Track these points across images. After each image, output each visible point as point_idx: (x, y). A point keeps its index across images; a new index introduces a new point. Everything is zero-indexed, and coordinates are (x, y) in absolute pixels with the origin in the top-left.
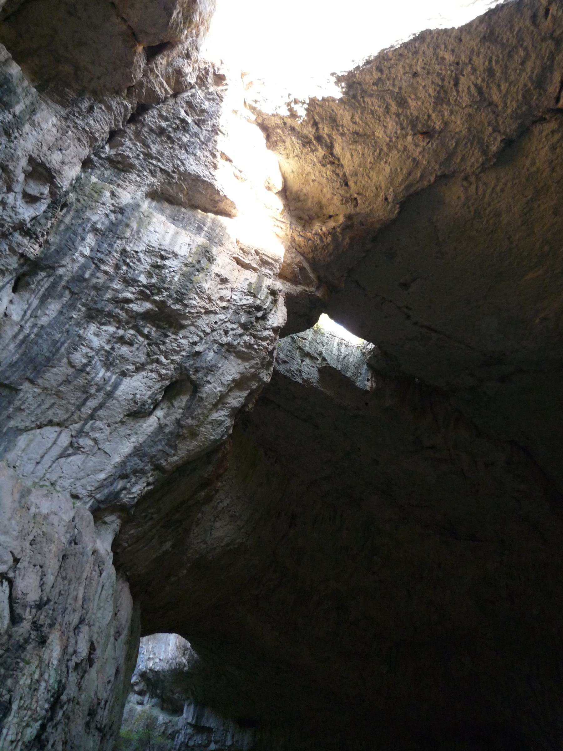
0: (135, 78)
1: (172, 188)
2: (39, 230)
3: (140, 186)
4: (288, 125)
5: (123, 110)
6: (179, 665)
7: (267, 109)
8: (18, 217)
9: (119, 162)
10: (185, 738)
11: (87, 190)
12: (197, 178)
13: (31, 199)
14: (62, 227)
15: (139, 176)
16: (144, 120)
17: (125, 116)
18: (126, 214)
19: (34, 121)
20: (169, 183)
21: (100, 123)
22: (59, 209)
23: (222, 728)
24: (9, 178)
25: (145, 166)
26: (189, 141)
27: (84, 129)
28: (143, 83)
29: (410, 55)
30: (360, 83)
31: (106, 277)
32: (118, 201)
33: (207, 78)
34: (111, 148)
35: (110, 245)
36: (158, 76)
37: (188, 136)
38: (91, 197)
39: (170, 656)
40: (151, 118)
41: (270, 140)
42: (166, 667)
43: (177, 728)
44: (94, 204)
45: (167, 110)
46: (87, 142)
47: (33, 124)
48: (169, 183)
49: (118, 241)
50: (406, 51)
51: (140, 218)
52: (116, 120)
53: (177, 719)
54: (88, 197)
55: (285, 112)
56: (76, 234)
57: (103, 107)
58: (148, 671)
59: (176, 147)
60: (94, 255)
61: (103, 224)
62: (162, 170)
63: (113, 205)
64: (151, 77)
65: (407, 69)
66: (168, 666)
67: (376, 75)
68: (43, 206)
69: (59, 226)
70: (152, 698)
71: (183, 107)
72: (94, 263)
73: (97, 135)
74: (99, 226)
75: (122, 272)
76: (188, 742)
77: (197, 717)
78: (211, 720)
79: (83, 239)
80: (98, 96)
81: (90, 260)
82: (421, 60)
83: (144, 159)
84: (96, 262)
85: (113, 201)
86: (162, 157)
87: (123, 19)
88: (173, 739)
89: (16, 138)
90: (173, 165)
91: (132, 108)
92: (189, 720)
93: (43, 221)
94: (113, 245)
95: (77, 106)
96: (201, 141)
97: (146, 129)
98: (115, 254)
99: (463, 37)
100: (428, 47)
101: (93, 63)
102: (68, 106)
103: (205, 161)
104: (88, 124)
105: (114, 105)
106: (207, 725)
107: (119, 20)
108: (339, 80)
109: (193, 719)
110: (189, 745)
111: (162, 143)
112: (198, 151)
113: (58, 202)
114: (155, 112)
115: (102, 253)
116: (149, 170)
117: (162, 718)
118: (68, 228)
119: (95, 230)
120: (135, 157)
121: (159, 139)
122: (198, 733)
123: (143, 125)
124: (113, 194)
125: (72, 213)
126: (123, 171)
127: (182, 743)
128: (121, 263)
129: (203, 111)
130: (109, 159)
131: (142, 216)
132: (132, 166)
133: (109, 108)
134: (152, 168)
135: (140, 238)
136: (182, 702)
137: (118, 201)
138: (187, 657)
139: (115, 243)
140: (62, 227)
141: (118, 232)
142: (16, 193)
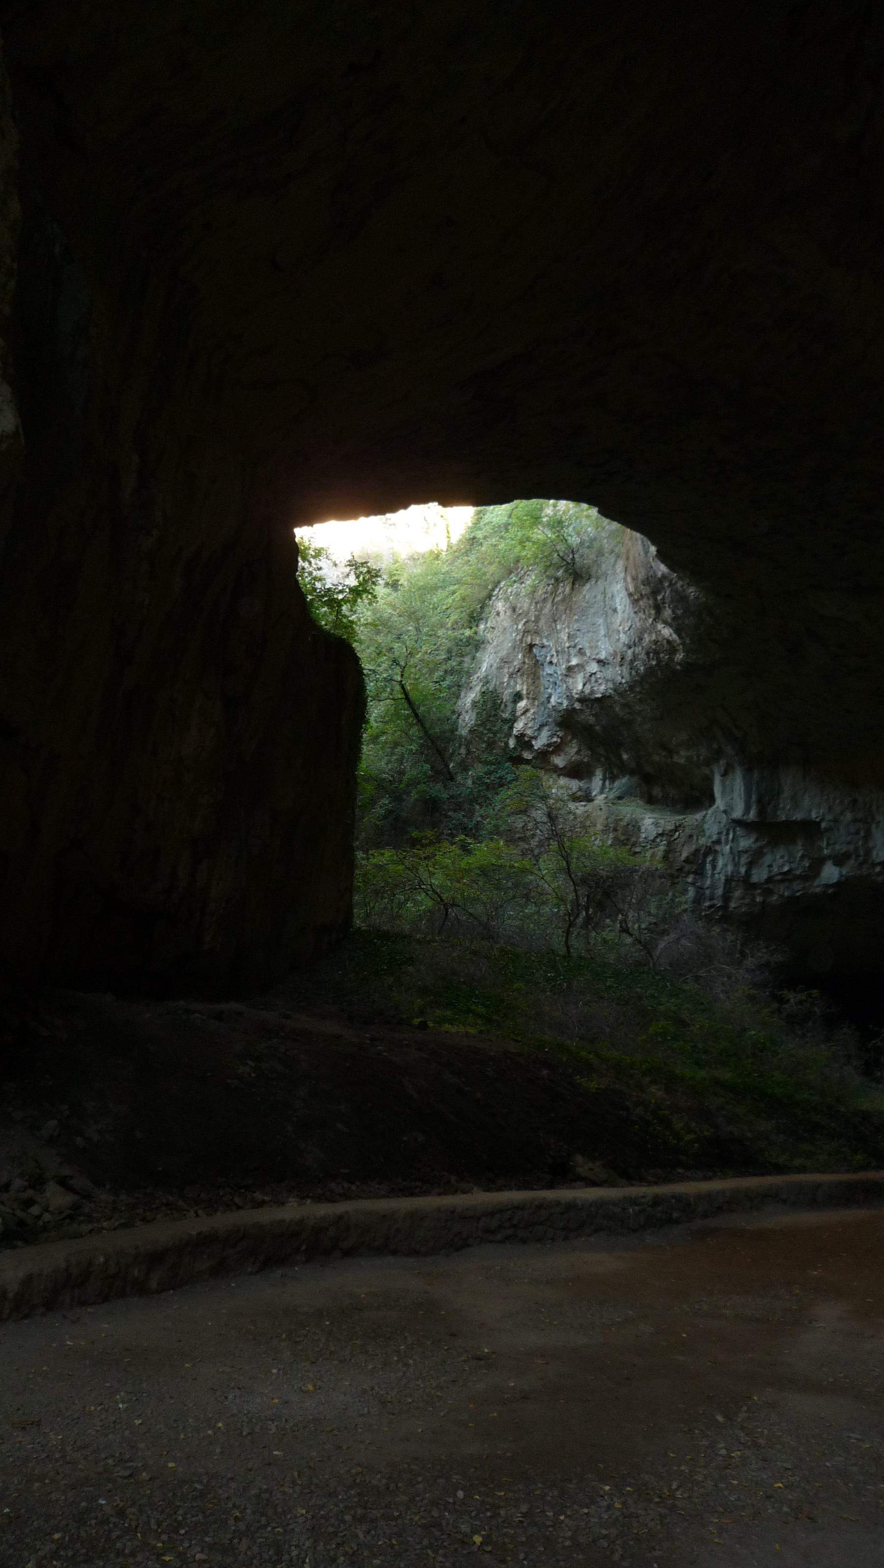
6: (656, 653)
10: (736, 865)
23: (849, 816)
39: (623, 638)
42: (618, 674)
43: (703, 841)
53: (698, 816)
58: (577, 706)
66: (625, 670)
70: (613, 779)
76: (748, 874)
77: (759, 801)
78: (806, 802)
88: (700, 872)
92: (738, 814)
106: (798, 816)
109: (747, 809)
110: (755, 879)
117: (651, 823)
122: (774, 843)
127: (728, 881)
136: (706, 771)
138: (667, 613)
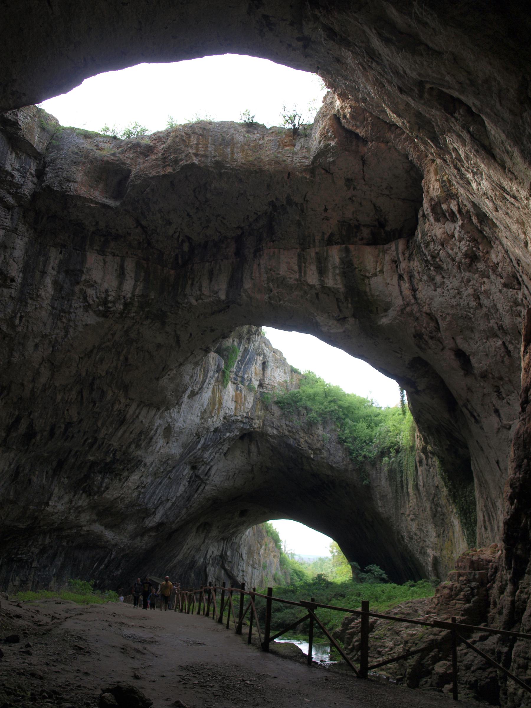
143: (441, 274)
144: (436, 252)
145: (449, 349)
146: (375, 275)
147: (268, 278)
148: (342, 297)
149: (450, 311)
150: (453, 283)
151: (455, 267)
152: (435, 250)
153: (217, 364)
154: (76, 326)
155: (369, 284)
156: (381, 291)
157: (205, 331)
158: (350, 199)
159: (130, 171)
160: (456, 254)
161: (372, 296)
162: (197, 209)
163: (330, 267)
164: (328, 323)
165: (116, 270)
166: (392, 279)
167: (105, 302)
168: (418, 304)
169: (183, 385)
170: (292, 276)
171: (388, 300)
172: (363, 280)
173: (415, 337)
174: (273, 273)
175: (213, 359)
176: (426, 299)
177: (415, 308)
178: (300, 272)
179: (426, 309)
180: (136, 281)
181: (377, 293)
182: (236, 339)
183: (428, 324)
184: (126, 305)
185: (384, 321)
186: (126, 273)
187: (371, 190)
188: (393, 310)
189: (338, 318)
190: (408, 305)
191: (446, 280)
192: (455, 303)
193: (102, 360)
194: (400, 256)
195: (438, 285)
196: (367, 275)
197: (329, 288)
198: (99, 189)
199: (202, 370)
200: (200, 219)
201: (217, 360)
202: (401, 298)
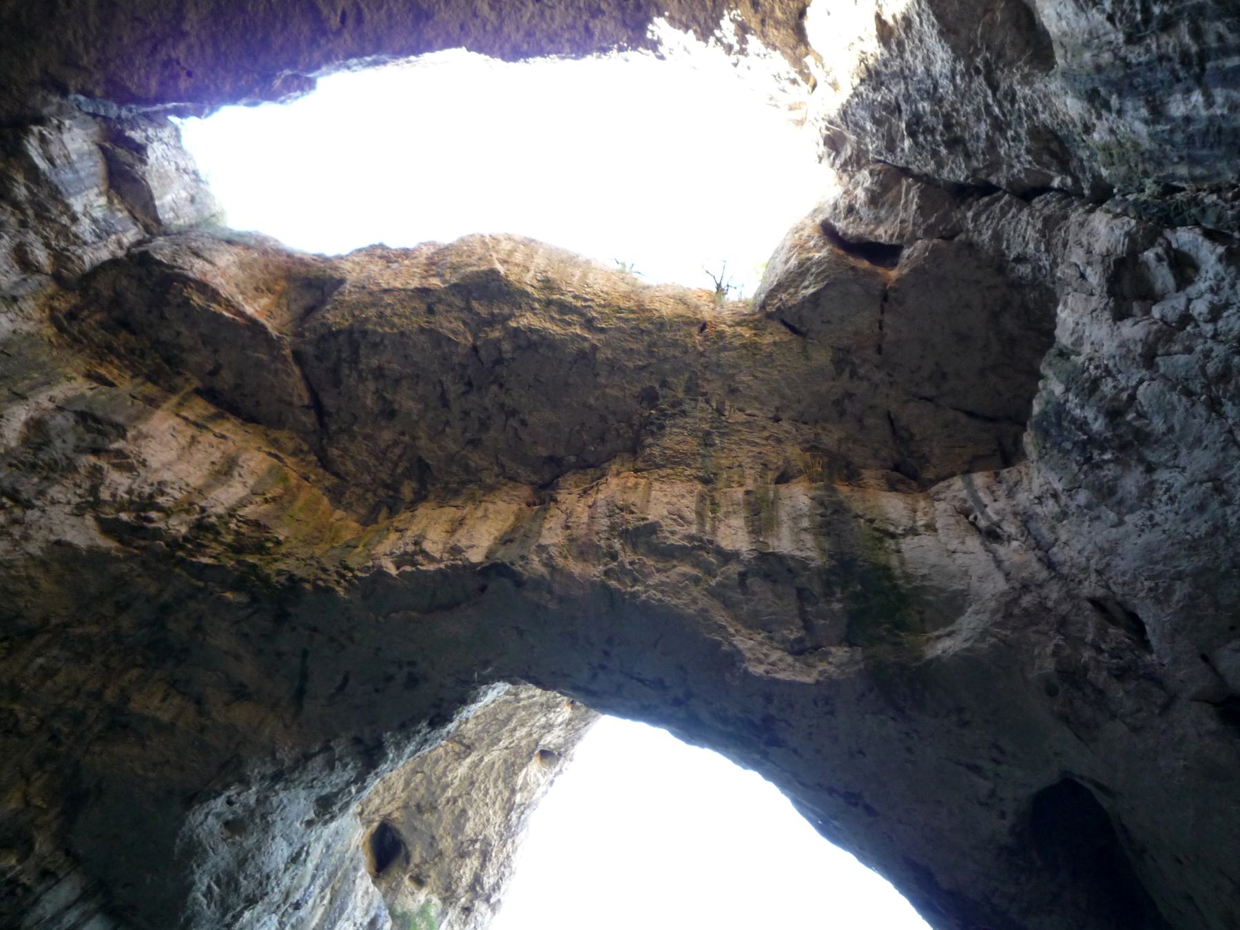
0: (926, 249)
1: (1003, 44)
2: (1230, 213)
3: (1045, 96)
4: (759, 17)
5: (983, 218)
7: (779, 63)
8: (1222, 273)
9: (1052, 154)
11: (1123, 170)
12: (947, 31)
13: (1184, 267)
14: (1199, 171)
15: (1036, 111)
16: (967, 178)
17: (988, 205)
18: (1089, 86)
19: (1073, 344)
20: (1000, 56)
21: (1022, 230)
22: (1179, 196)
24: (1158, 339)
25: (1014, 117)
26: (922, 99)
27: (1047, 250)
28: (925, 230)
29: (538, 35)
30: (625, 24)
31: (1205, 25)
32: (1086, 116)
33: (850, 157)
34: (1052, 178)
35: (1149, 66)
36: (902, 222)
37: (920, 106)
38: (1124, 159)
40: (957, 172)
41: (801, 6)
44: (1128, 145)
45: (926, 165)
46: (1060, 230)
47: (1079, 342)
48: (1000, 56)
49: (1134, 61)
50: (543, 43)
51: (1073, 56)
52: (1004, 213)
54: (1128, 162)
55: (754, 42)
56: (1190, 140)
57: (1004, 246)
59: (946, 106)
60: (1191, 82)
61: (1136, 109)
62: (995, 89)
63: (1099, 117)
64: (910, 228)
65: (548, 13)
67: (596, 25)
68: (1185, 237)
69: (1203, 179)
71: (903, 150)
72: (1203, 69)
73: (1039, 225)
74: (1144, 112)
75: (1166, 8)
79: (1188, 120)
80: (1000, 264)
81: (1206, 79)
82: (525, 19)
83: (1009, 125)
84: (1197, 69)
85: (1095, 121)
86: (979, 108)
87: (881, 328)
89: (1097, 368)
90: (971, 82)
91: (969, 208)
93: (1211, 215)
94: (1148, 63)
95: (1035, 278)
96: (906, 84)
97: (975, 164)
98: (1154, 46)
99: (457, 30)
100: (509, 36)
101: (968, 306)
102: (1048, 289)
103: (918, 48)
104: (1037, 249)
105: (987, 235)
107: (886, 330)
108: (654, 45)
111: (966, 127)
112: (919, 71)
113: (1162, 215)
114: (945, 173)
115: (1173, 72)
116: (1013, 105)
118: (1193, 161)
119: (1157, 113)
120: (1021, 141)
121: (967, 136)
123: (975, 171)
124: (1088, 129)
125: (1170, 170)
126: (1056, 137)
128: (1154, 24)
129: (877, 122)
130: (1064, 169)
131: (1069, 55)
132: (1034, 133)
133: (997, 237)
134: (1007, 105)
135: (1090, 33)
137: (1086, 116)
139: (1139, 64)
140: (1199, 171)
141: (1121, 73)
142: (1189, 301)
143: (1141, 460)
144: (1124, 396)
145: (1195, 699)
146: (912, 531)
147: (612, 527)
148: (817, 589)
149: (1185, 565)
150: (1182, 474)
151: (1201, 410)
152: (1123, 390)
153: (372, 914)
154: (26, 538)
155: (899, 551)
156: (934, 566)
157: (390, 678)
158: (837, 403)
159: (341, 281)
160: (1207, 355)
161: (908, 577)
162: (470, 384)
163: (785, 518)
164: (766, 656)
165: (213, 463)
166: (963, 543)
167: (145, 504)
168: (1061, 577)
169: (260, 870)
170: (678, 528)
171: (957, 586)
172: (880, 540)
173: (1052, 692)
174: (629, 517)
175: (367, 892)
176: (1088, 560)
177: (1054, 592)
178: (702, 524)
179: (1090, 587)
180: (254, 493)
181: (925, 571)
182: (435, 900)
183: (1102, 632)
184: (201, 527)
185: (945, 646)
186: (235, 473)
187: (891, 384)
188: (977, 613)
189: (797, 648)
190: (1025, 588)
191: (1162, 475)
192: (1204, 528)
193: (47, 673)
194: (981, 494)
195: (1129, 502)
196: (892, 529)
197: (780, 558)
198: (256, 306)
199: (328, 897)
200: (466, 413)
201: (375, 904)
202: (999, 579)
